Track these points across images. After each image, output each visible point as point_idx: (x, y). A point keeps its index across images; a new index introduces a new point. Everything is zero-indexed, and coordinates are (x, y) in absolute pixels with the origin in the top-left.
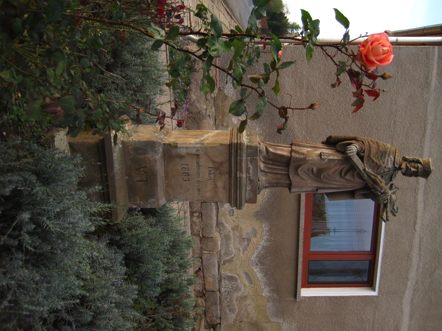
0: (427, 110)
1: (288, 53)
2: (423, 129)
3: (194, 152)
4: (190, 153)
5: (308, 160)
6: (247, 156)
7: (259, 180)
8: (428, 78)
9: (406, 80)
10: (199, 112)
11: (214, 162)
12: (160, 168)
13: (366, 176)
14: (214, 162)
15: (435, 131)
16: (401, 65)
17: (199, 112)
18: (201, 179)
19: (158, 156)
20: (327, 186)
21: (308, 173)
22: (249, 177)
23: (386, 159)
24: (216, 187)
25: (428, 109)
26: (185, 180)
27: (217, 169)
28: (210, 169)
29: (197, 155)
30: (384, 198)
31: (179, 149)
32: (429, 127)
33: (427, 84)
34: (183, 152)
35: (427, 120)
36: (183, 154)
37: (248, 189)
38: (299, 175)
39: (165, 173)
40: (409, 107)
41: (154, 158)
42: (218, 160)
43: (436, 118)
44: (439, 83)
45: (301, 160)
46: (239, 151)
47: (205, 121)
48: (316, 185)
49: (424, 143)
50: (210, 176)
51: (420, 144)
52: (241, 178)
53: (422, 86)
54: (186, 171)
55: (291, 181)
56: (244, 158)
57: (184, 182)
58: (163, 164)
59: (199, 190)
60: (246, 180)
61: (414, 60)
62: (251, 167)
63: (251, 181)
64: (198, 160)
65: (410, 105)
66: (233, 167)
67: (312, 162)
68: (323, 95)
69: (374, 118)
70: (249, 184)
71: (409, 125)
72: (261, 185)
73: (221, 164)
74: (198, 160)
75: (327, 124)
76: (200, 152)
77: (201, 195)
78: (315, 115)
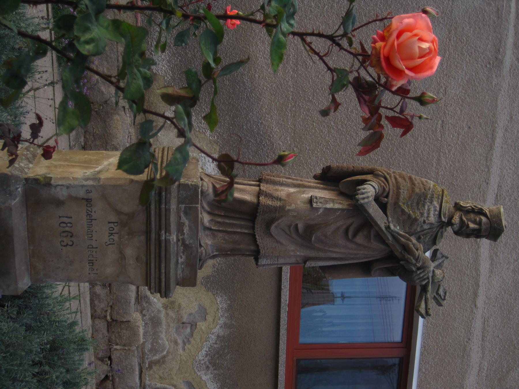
0: (496, 106)
2: (490, 136)
3: (82, 194)
4: (74, 196)
5: (289, 210)
6: (180, 201)
7: (201, 246)
8: (499, 50)
9: (463, 54)
10: (106, 101)
11: (119, 213)
12: (18, 223)
13: (390, 238)
14: (119, 213)
15: (510, 141)
16: (456, 28)
17: (106, 101)
19: (15, 202)
20: (321, 255)
21: (288, 232)
22: (183, 239)
23: (426, 208)
24: (122, 257)
26: (65, 244)
27: (123, 224)
29: (87, 200)
30: (421, 275)
31: (53, 190)
32: (500, 134)
33: (498, 62)
34: (62, 194)
35: (496, 122)
36: (62, 198)
37: (180, 260)
38: (272, 236)
39: (28, 231)
40: (468, 99)
41: (7, 205)
42: (126, 209)
43: (512, 118)
45: (276, 210)
46: (164, 193)
47: (116, 117)
48: (302, 254)
49: (491, 160)
50: (112, 237)
51: (485, 162)
52: (167, 241)
53: (489, 63)
54: (67, 229)
55: (257, 246)
56: (173, 206)
57: (63, 248)
58: (25, 215)
59: (91, 263)
60: (178, 245)
61: (476, 20)
62: (187, 223)
63: (186, 247)
64: (89, 209)
65: (468, 96)
66: (153, 223)
67: (295, 214)
68: (323, 76)
70: (183, 253)
71: (466, 129)
72: (204, 254)
73: (132, 216)
74: (89, 209)
75: (328, 126)
76: (94, 195)
77: (95, 271)
78: (308, 110)
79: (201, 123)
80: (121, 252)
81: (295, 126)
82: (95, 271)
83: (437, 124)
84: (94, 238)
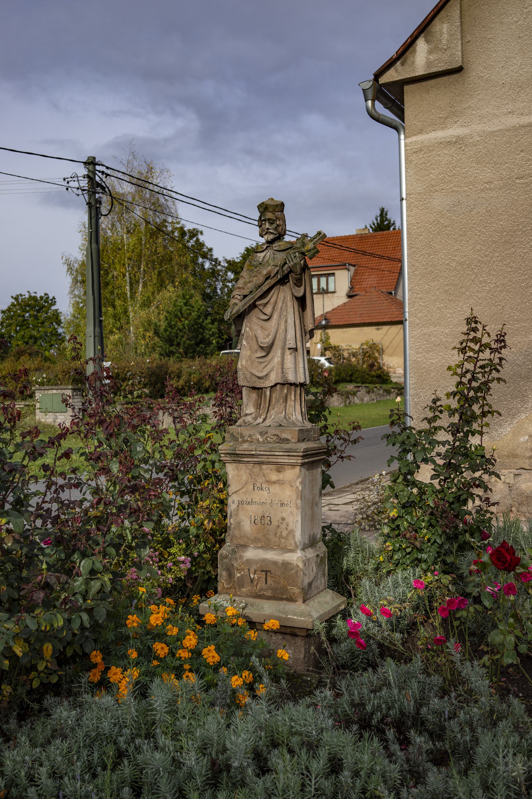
1: (419, 358)
8: (449, 142)
9: (454, 175)
18: (269, 501)
21: (265, 364)
25: (496, 129)
26: (269, 523)
28: (256, 488)
35: (514, 126)
38: (267, 375)
43: (510, 112)
44: (456, 122)
55: (276, 385)
61: (425, 169)
69: (514, 212)
77: (289, 503)
78: (511, 308)
79: (527, 408)
80: (274, 483)
81: (528, 319)
82: (289, 503)
83: (520, 183)
84: (265, 501)
